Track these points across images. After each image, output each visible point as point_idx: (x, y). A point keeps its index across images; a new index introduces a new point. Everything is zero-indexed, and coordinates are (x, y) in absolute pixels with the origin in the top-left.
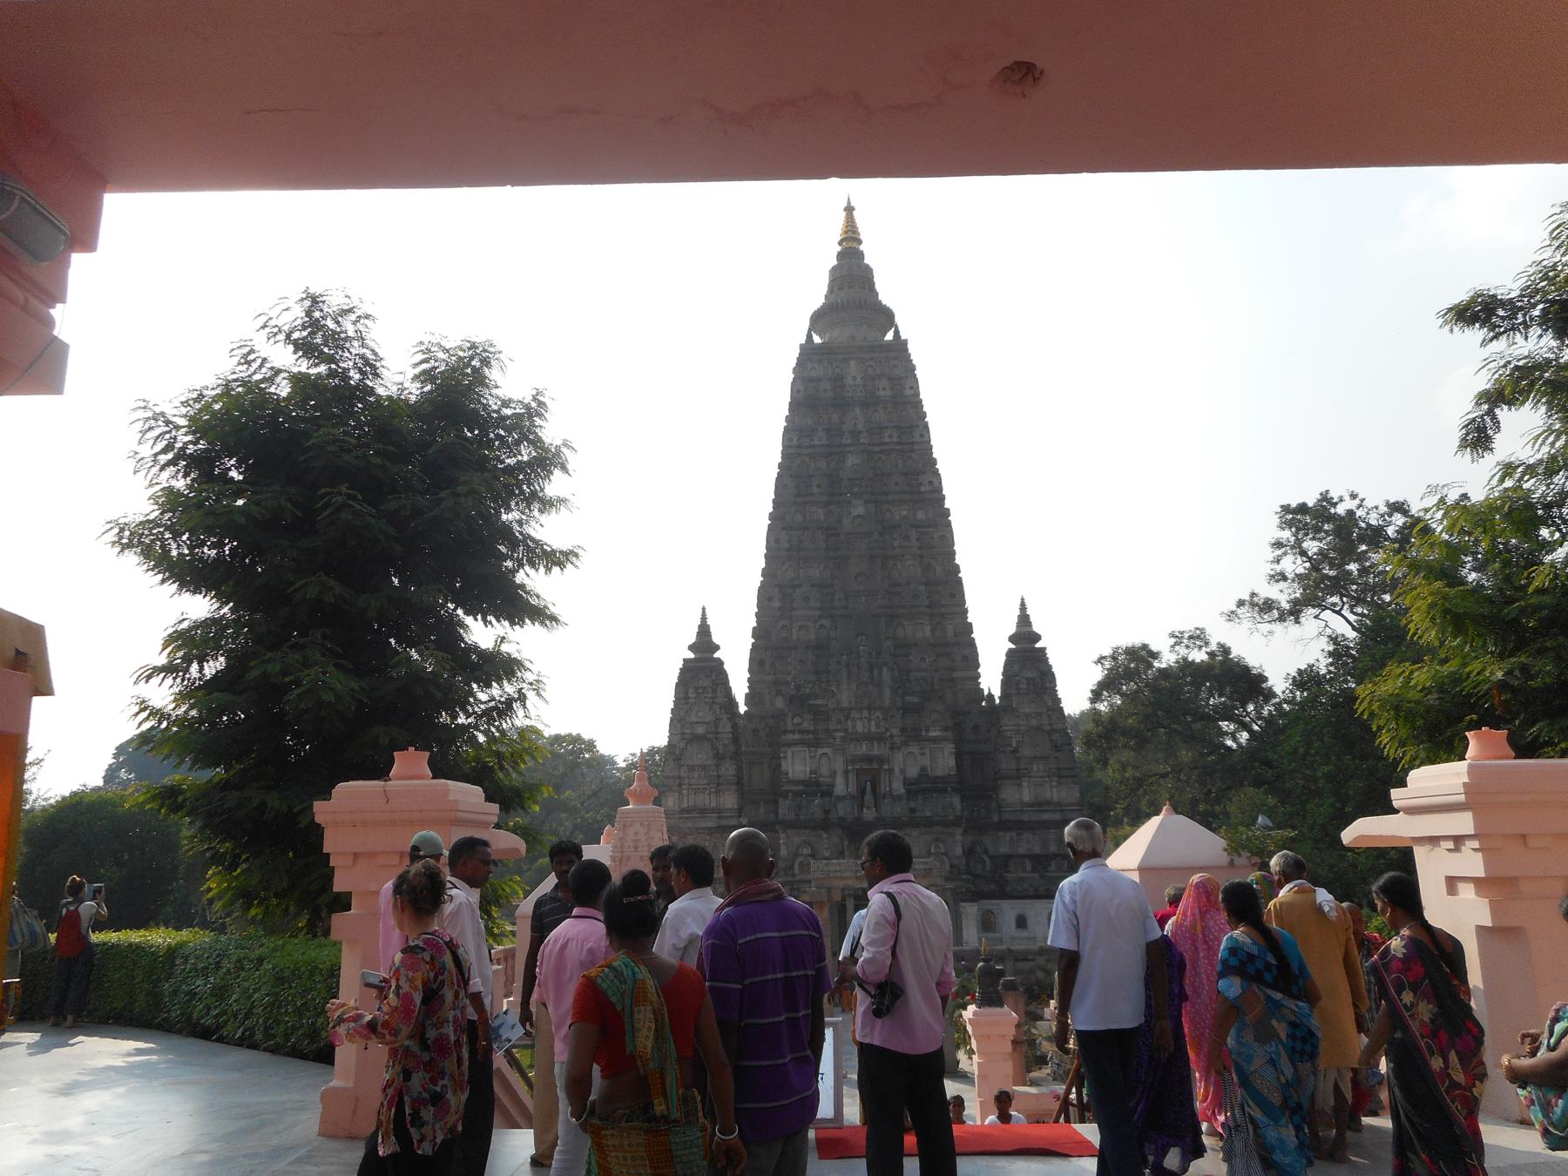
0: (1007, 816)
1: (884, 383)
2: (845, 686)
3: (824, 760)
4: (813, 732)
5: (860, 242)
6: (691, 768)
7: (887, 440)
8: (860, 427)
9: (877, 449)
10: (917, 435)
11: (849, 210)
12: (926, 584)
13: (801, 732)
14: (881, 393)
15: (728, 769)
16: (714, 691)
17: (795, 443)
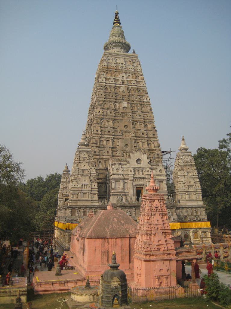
0: (181, 204)
1: (131, 67)
2: (132, 160)
3: (126, 184)
4: (123, 175)
5: (120, 24)
6: (82, 185)
7: (133, 84)
8: (125, 79)
9: (130, 87)
10: (141, 83)
11: (117, 14)
12: (146, 130)
13: (118, 175)
14: (131, 70)
15: (95, 185)
16: (89, 159)
17: (104, 81)
